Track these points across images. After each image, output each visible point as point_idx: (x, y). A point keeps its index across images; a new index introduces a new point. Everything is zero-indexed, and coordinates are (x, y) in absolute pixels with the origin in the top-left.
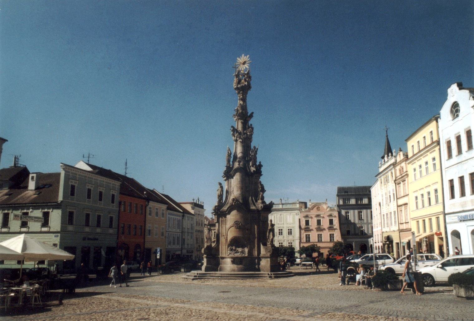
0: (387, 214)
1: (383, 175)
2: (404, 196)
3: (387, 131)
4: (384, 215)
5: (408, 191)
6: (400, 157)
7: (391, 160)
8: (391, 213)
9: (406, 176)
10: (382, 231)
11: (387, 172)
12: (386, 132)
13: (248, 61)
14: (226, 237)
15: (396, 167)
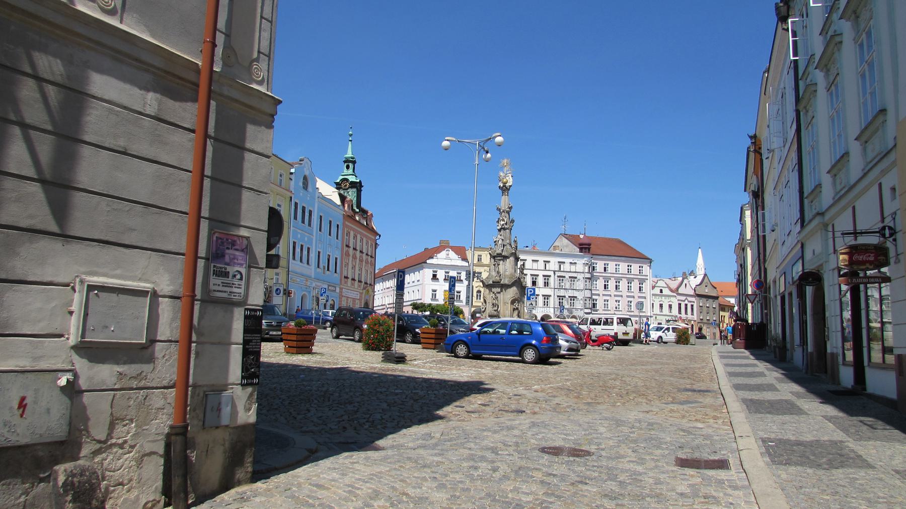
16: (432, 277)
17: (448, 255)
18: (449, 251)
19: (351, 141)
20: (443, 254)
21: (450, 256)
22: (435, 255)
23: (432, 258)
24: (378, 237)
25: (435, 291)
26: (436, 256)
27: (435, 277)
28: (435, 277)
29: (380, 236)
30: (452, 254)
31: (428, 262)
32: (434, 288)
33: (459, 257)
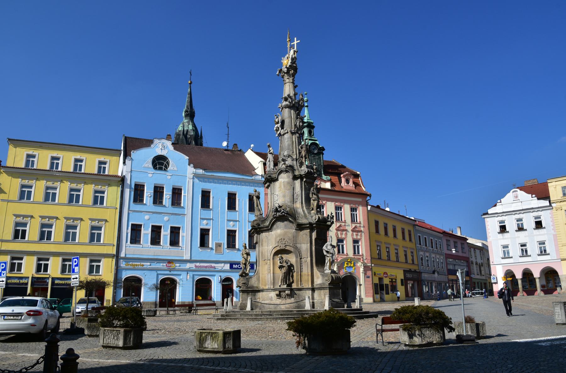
16: (498, 230)
17: (517, 197)
18: (517, 191)
19: (307, 106)
20: (509, 197)
21: (519, 198)
22: (499, 201)
23: (495, 206)
24: (368, 198)
25: (505, 247)
26: (501, 202)
27: (503, 229)
28: (503, 229)
29: (370, 197)
30: (522, 194)
31: (490, 211)
32: (505, 243)
33: (534, 196)
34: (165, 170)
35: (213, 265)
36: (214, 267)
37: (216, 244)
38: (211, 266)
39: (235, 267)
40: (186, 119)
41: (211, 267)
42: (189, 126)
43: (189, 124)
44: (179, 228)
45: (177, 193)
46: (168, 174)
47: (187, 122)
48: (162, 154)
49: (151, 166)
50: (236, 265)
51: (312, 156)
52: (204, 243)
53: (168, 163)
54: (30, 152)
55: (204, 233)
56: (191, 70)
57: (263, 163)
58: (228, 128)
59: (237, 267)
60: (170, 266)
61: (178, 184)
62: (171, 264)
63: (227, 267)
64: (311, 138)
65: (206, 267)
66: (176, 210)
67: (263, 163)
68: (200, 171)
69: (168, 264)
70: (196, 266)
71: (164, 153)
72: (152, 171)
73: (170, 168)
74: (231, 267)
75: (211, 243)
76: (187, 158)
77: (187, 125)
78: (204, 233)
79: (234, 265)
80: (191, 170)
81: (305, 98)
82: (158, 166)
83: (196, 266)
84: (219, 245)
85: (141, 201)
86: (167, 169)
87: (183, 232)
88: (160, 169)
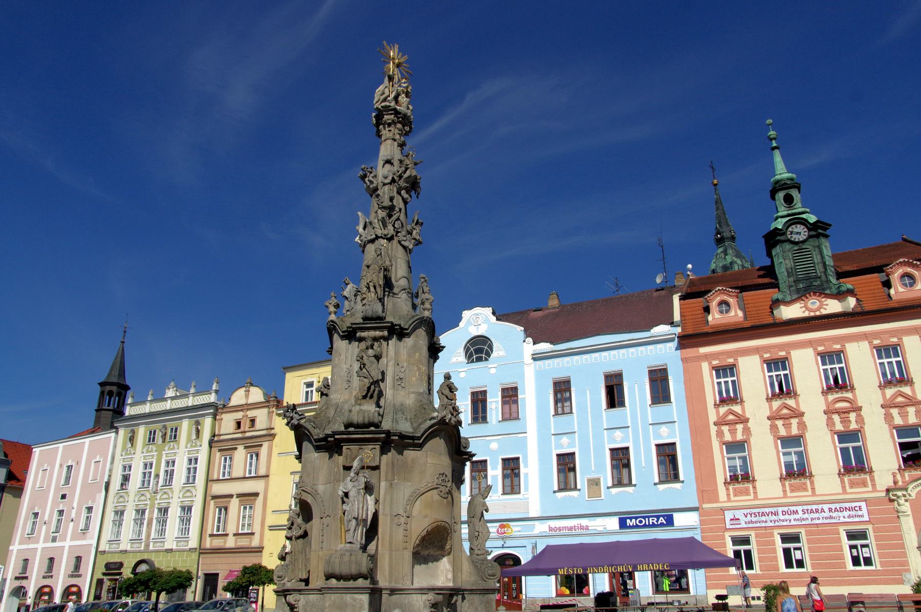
0: (141, 512)
1: (146, 423)
2: (245, 478)
3: (125, 332)
4: (120, 513)
5: (268, 468)
6: (247, 396)
7: (194, 396)
8: (164, 511)
9: (268, 438)
10: (101, 548)
11: (181, 419)
12: (123, 333)
13: (405, 67)
14: (402, 520)
15: (222, 413)
34: (486, 360)
35: (584, 522)
36: (587, 528)
37: (589, 481)
38: (581, 526)
39: (631, 524)
40: (720, 247)
41: (582, 528)
42: (727, 257)
43: (726, 255)
44: (517, 459)
45: (510, 395)
46: (490, 366)
47: (722, 252)
48: (479, 334)
49: (462, 358)
50: (634, 520)
51: (796, 248)
52: (566, 484)
53: (491, 347)
54: (309, 380)
55: (566, 463)
56: (711, 162)
57: (679, 296)
58: (662, 247)
59: (635, 524)
60: (505, 533)
61: (509, 382)
62: (506, 529)
63: (613, 523)
64: (790, 212)
65: (570, 529)
66: (511, 426)
67: (679, 296)
68: (544, 347)
69: (500, 529)
70: (551, 529)
71: (481, 331)
72: (465, 367)
73: (494, 354)
74: (623, 524)
75: (581, 482)
76: (523, 328)
77: (723, 257)
78: (566, 463)
79: (628, 521)
80: (530, 348)
81: (770, 131)
82: (474, 357)
83: (551, 529)
84: (594, 483)
85: (484, 419)
86: (489, 356)
87: (526, 466)
88: (479, 359)
